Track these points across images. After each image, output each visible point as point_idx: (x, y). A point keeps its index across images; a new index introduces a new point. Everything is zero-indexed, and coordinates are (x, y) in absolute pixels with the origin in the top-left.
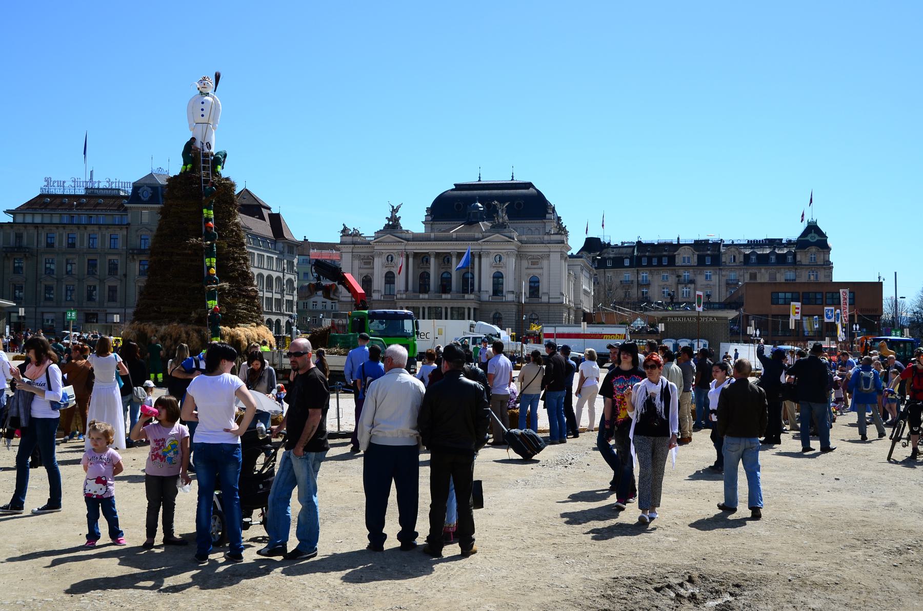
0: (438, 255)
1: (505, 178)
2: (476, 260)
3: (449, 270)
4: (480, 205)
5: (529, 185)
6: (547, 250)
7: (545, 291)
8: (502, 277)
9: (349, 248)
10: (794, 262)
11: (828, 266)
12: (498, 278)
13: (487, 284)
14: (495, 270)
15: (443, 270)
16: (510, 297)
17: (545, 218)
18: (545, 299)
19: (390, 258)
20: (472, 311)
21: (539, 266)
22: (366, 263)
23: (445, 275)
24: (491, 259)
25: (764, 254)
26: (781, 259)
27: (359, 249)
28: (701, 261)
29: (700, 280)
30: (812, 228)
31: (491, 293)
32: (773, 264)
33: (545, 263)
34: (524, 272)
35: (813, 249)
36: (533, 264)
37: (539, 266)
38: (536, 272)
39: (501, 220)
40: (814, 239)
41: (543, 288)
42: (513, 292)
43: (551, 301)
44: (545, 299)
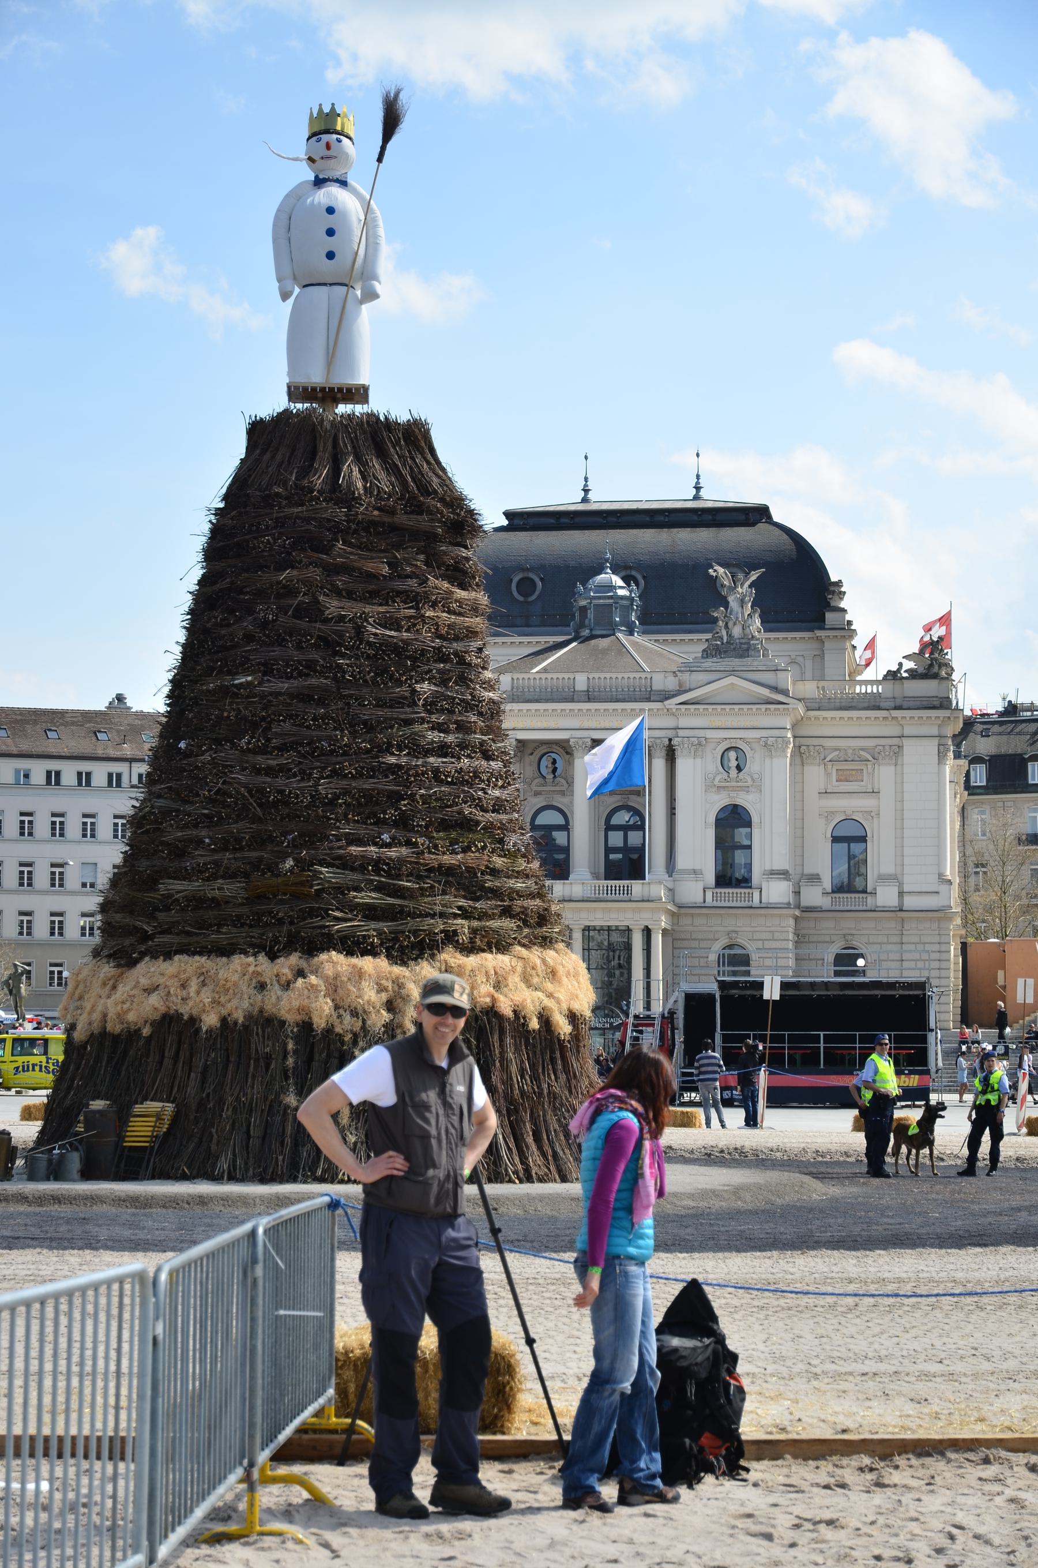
1: (675, 493)
2: (659, 765)
3: (559, 801)
4: (617, 581)
5: (761, 513)
6: (894, 731)
7: (888, 869)
8: (749, 824)
13: (698, 849)
14: (722, 800)
16: (777, 892)
17: (823, 619)
18: (886, 896)
20: (658, 940)
21: (866, 785)
23: (549, 818)
24: (710, 762)
31: (711, 878)
33: (885, 774)
34: (814, 804)
37: (866, 785)
38: (853, 805)
39: (737, 631)
41: (880, 857)
42: (784, 874)
43: (909, 902)
44: (886, 896)
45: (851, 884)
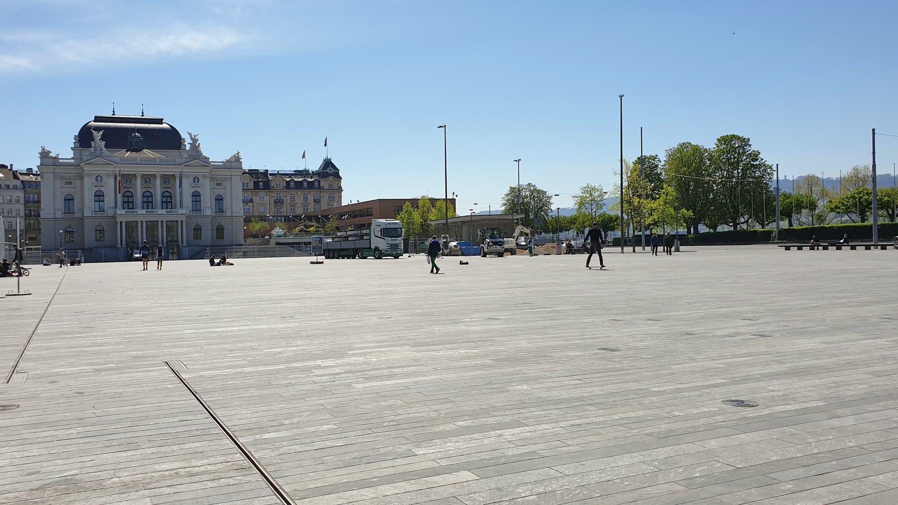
0: (143, 176)
9: (50, 169)
10: (320, 188)
11: (340, 189)
12: (196, 196)
13: (188, 200)
15: (145, 190)
18: (228, 213)
19: (99, 178)
20: (184, 224)
22: (67, 183)
25: (300, 182)
26: (311, 185)
27: (59, 170)
28: (256, 186)
29: (256, 199)
30: (328, 163)
32: (305, 189)
33: (228, 183)
35: (331, 178)
36: (218, 184)
38: (220, 191)
40: (329, 171)
41: (227, 204)
45: (221, 210)
